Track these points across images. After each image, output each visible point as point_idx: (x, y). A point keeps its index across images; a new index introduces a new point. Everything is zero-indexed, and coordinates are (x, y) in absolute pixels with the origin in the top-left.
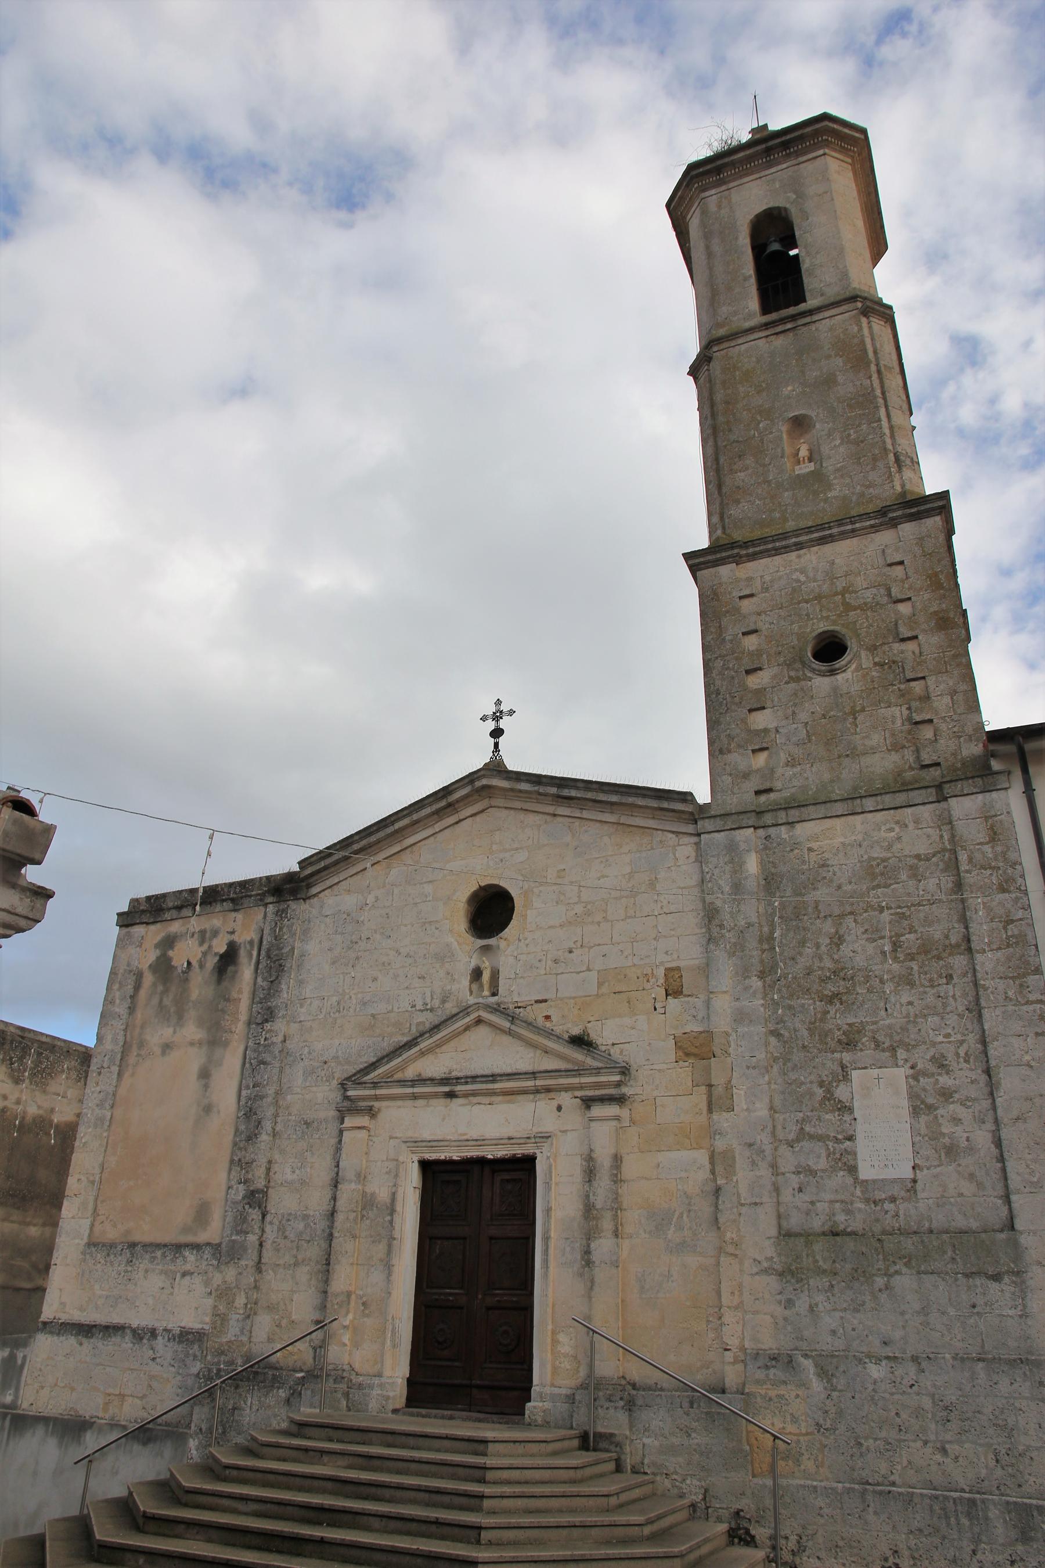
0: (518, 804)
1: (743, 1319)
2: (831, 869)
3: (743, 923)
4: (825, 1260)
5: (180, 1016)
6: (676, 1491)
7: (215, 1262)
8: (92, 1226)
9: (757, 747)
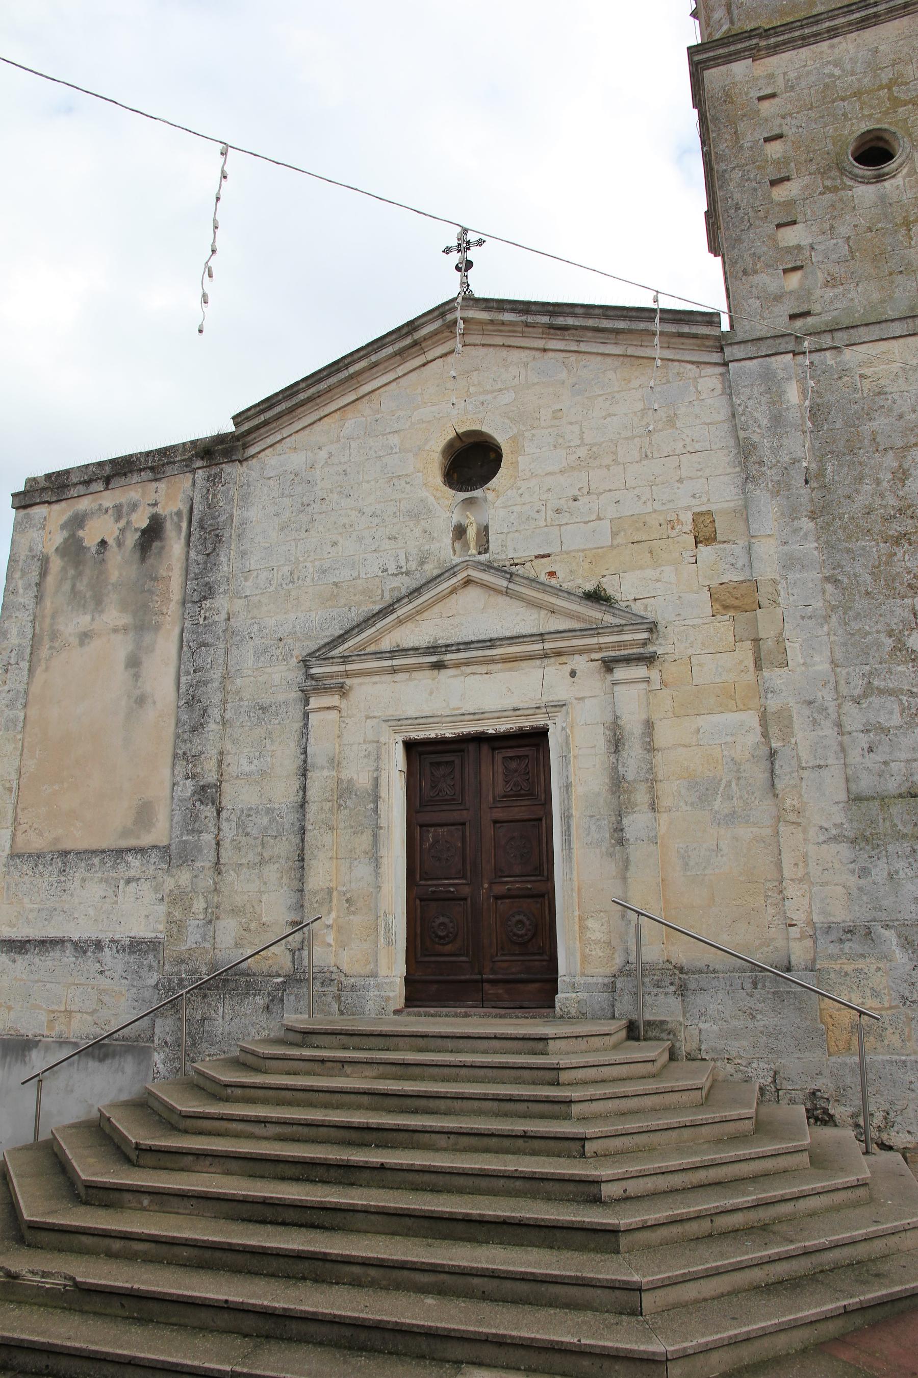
0: (499, 340)
1: (810, 892)
2: (889, 397)
3: (787, 459)
4: (905, 824)
5: (99, 602)
6: (740, 1075)
7: (165, 866)
8: (14, 836)
9: (789, 266)
